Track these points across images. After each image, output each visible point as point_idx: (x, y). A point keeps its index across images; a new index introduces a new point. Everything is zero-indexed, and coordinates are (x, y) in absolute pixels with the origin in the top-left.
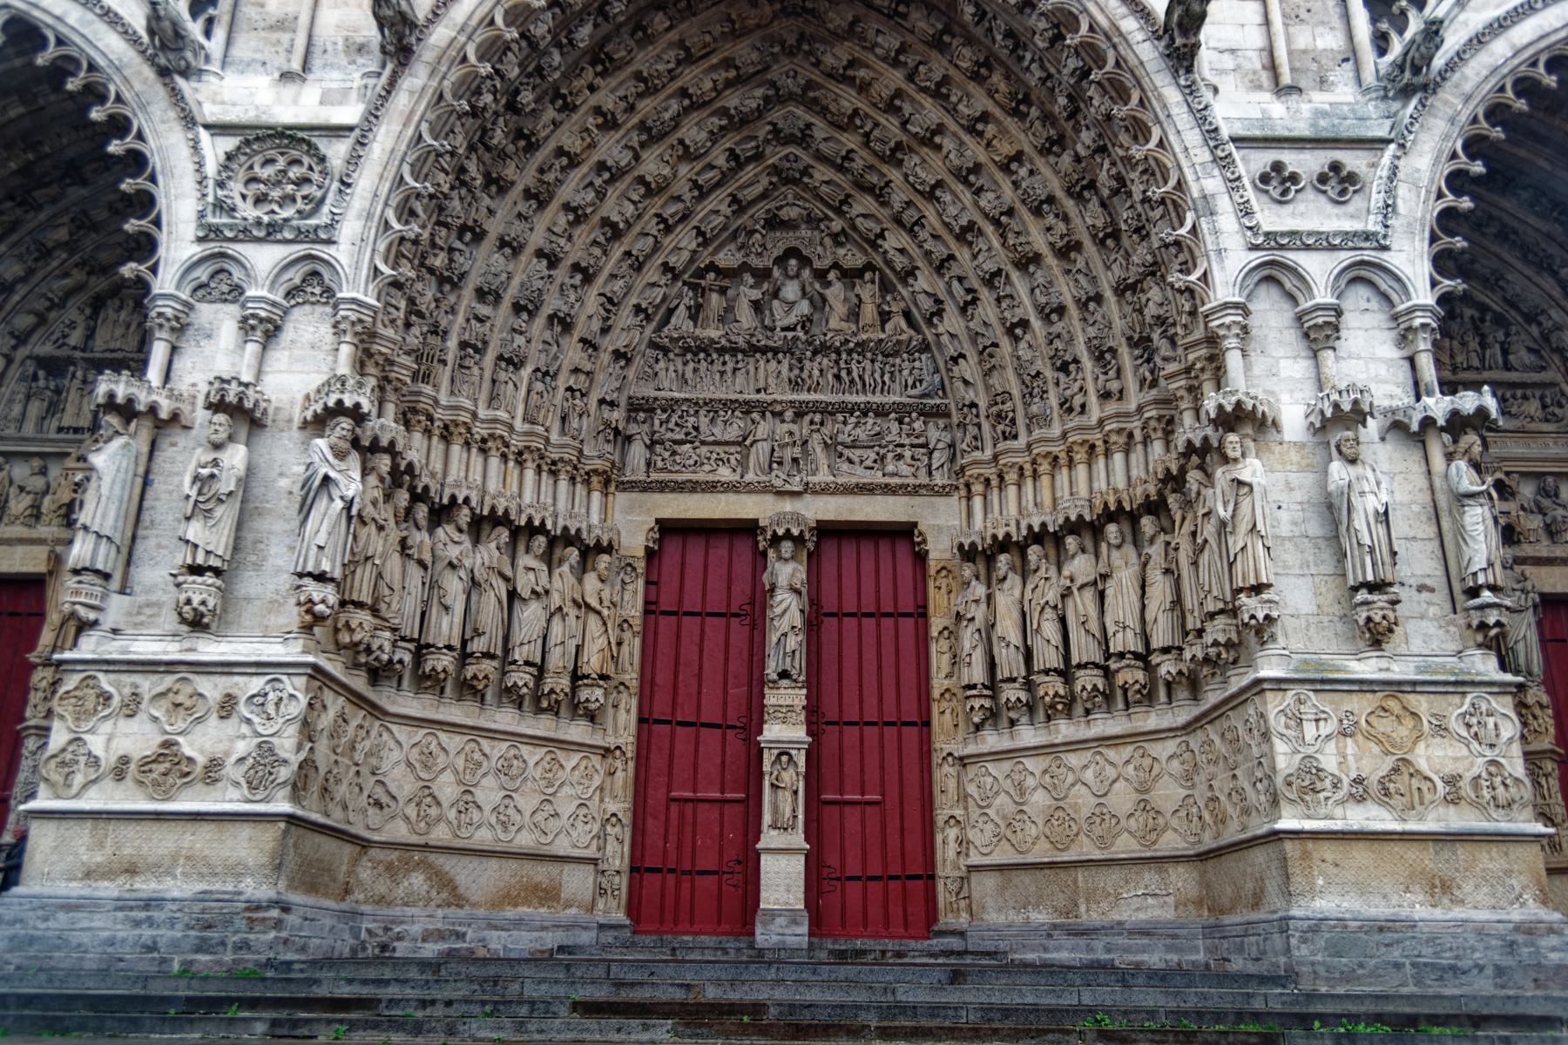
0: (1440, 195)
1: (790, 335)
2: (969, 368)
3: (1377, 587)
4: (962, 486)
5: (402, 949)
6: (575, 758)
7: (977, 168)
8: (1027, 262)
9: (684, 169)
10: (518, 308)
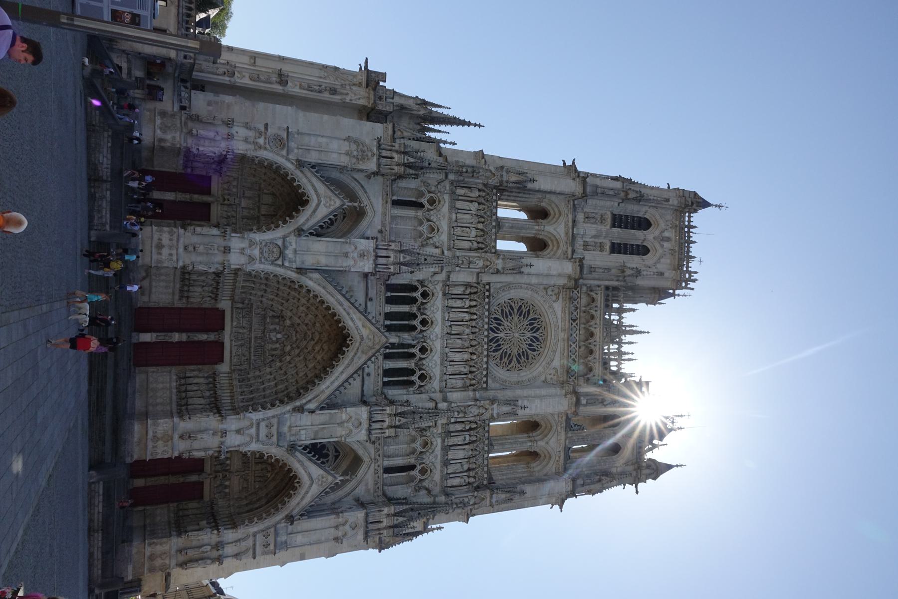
0: (267, 454)
1: (268, 336)
2: (257, 373)
3: (190, 437)
4: (232, 371)
5: (131, 274)
6: (171, 297)
7: (297, 374)
8: (276, 385)
9: (303, 315)
10: (266, 285)
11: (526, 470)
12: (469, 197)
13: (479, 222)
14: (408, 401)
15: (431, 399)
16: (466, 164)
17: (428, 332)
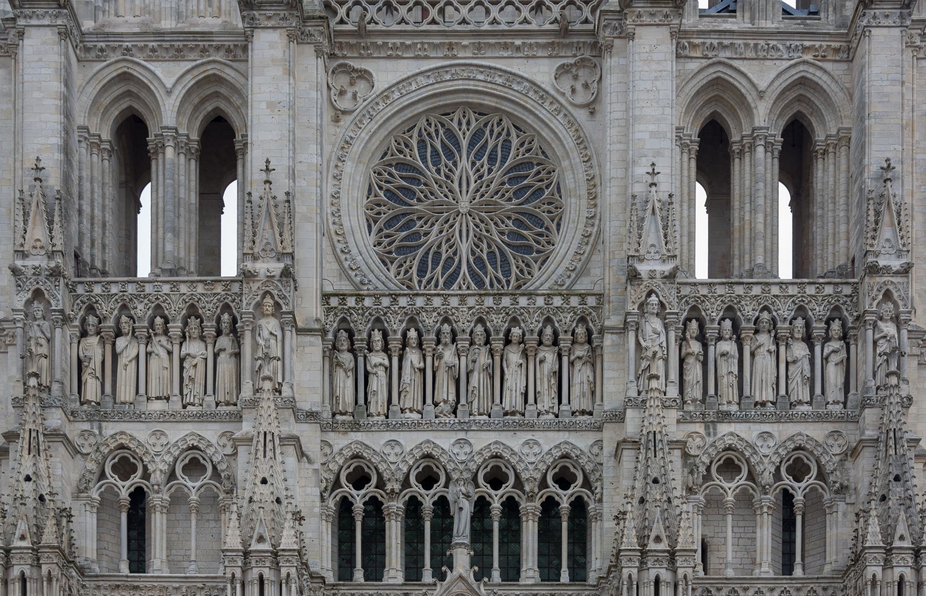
11: (831, 161)
12: (103, 363)
13: (166, 332)
14: (617, 517)
15: (617, 455)
16: (19, 376)
17: (450, 467)
